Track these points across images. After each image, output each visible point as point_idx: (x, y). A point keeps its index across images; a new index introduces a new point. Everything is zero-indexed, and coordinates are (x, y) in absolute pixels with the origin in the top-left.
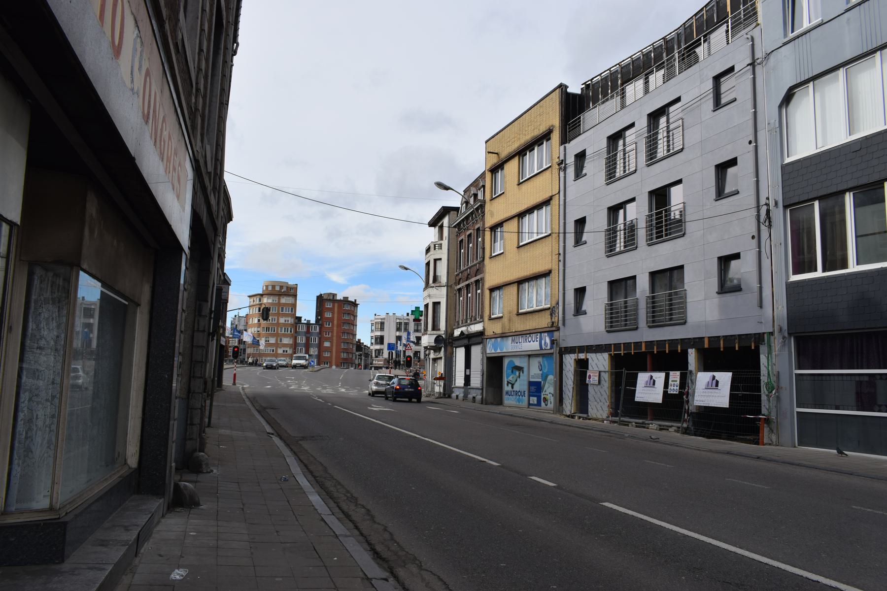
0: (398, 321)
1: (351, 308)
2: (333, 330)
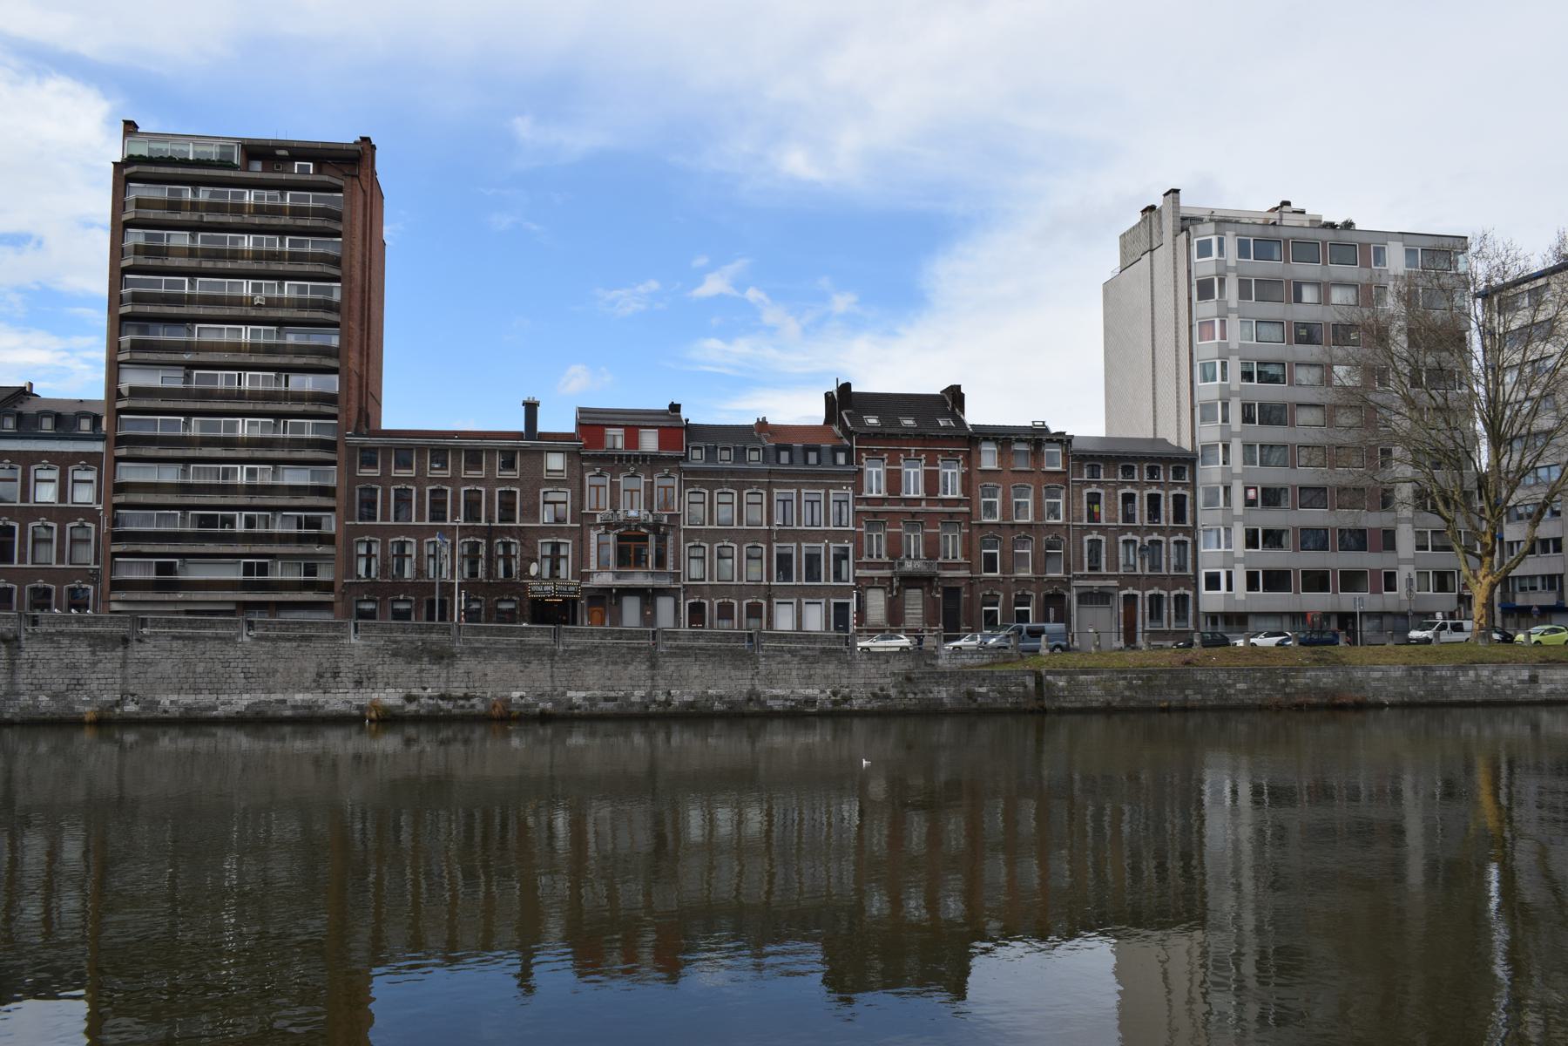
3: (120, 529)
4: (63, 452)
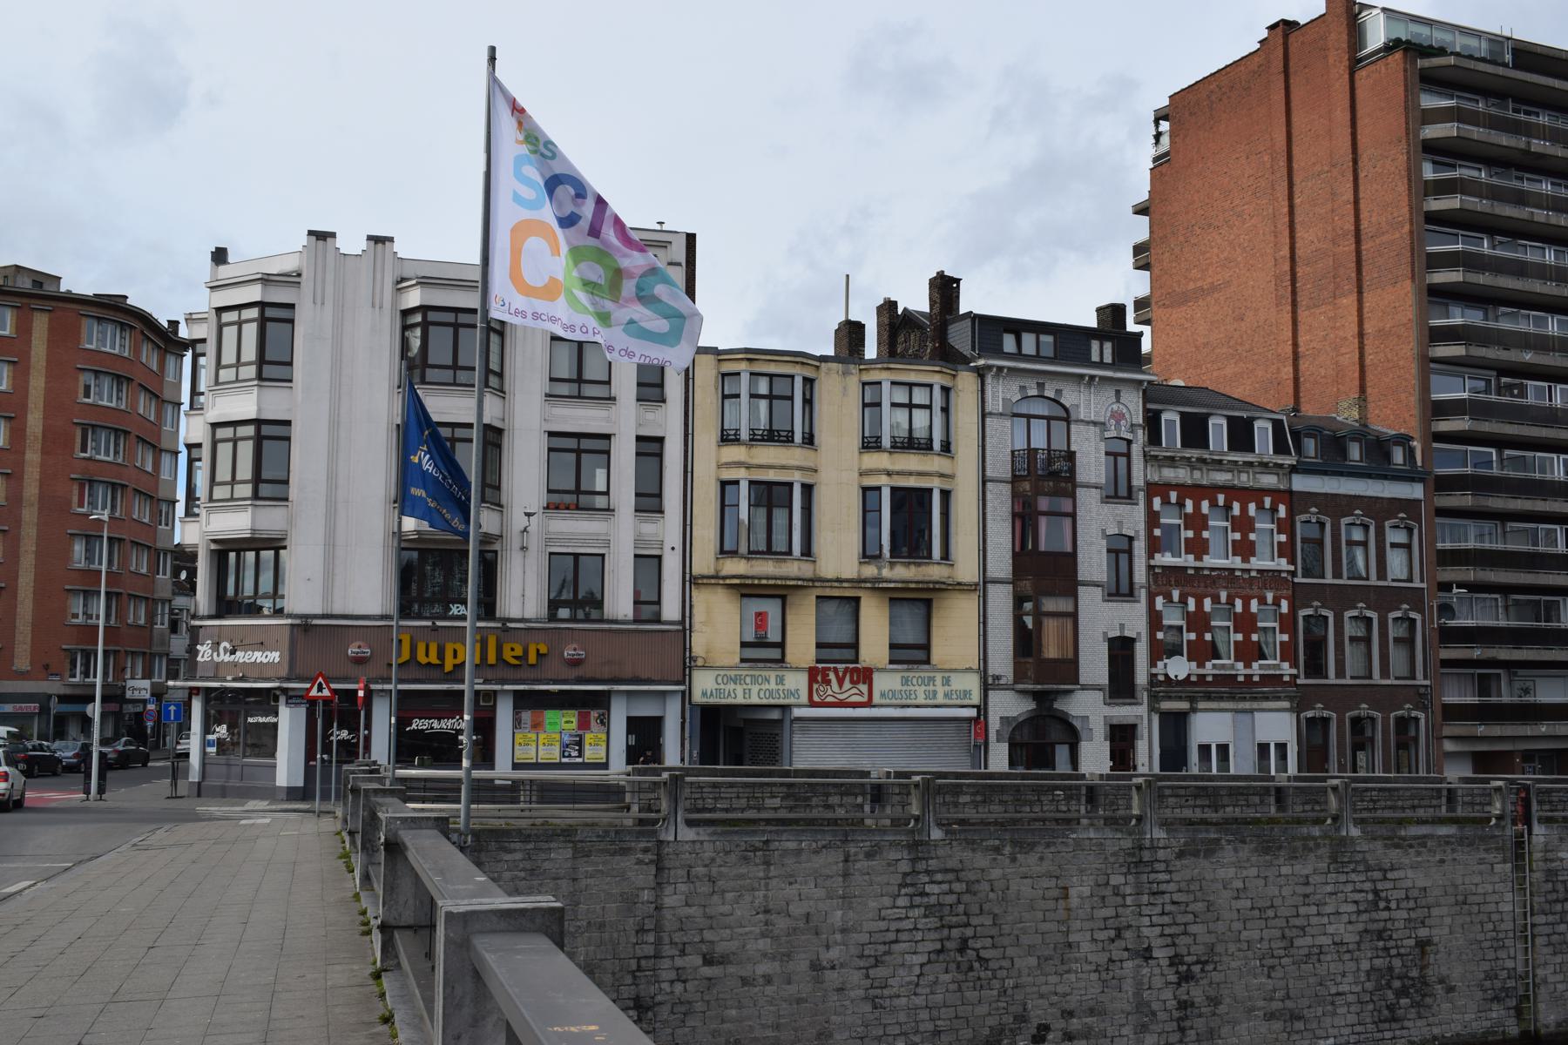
0: (414, 298)
1: (137, 351)
2: (20, 464)
3: (1453, 623)
4: (1377, 498)
